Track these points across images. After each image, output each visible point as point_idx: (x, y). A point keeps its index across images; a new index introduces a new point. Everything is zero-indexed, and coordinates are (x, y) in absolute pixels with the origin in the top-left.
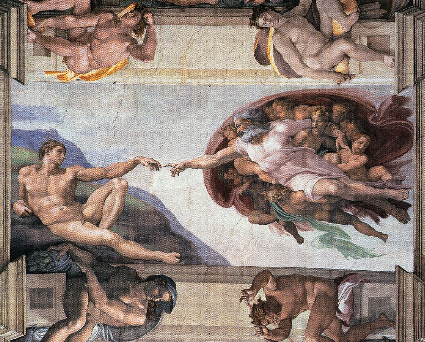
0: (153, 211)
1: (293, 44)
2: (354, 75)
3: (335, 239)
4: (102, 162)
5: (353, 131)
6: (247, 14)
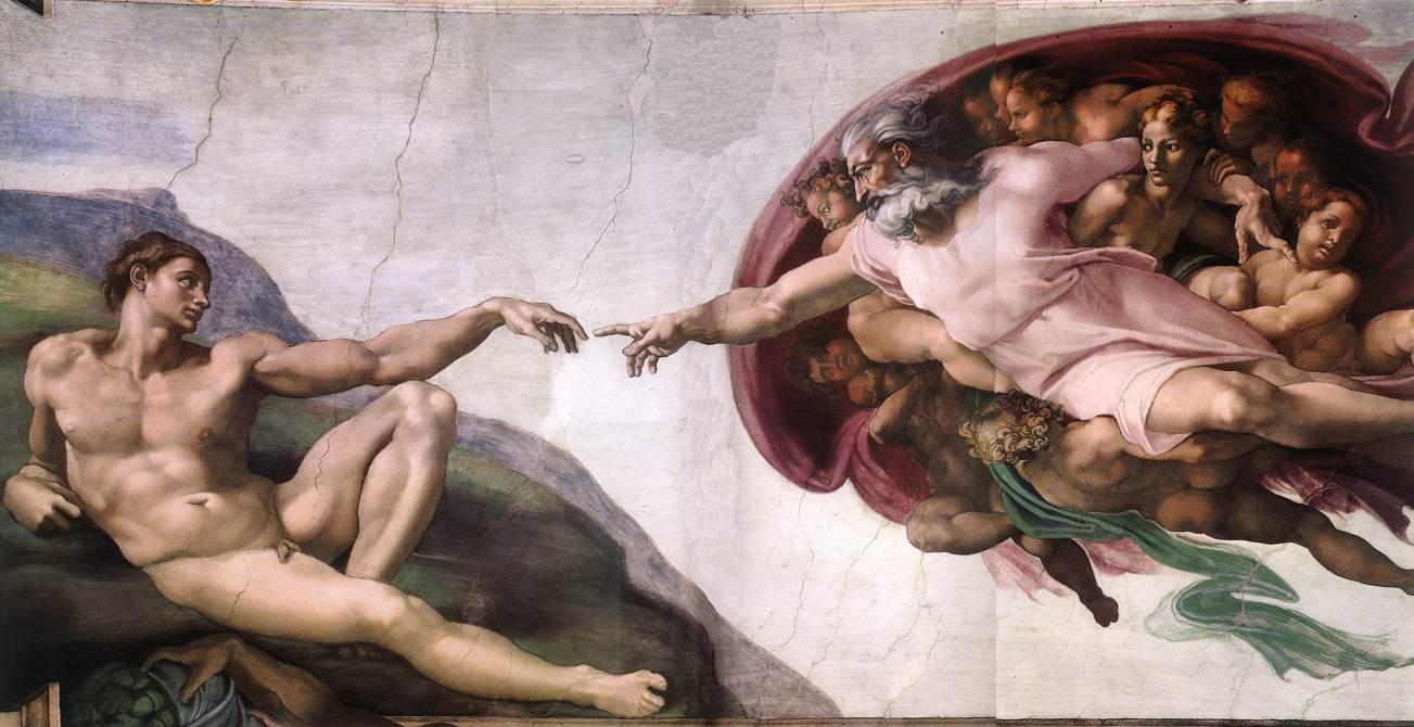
3: (1238, 605)
4: (353, 320)
5: (1299, 180)
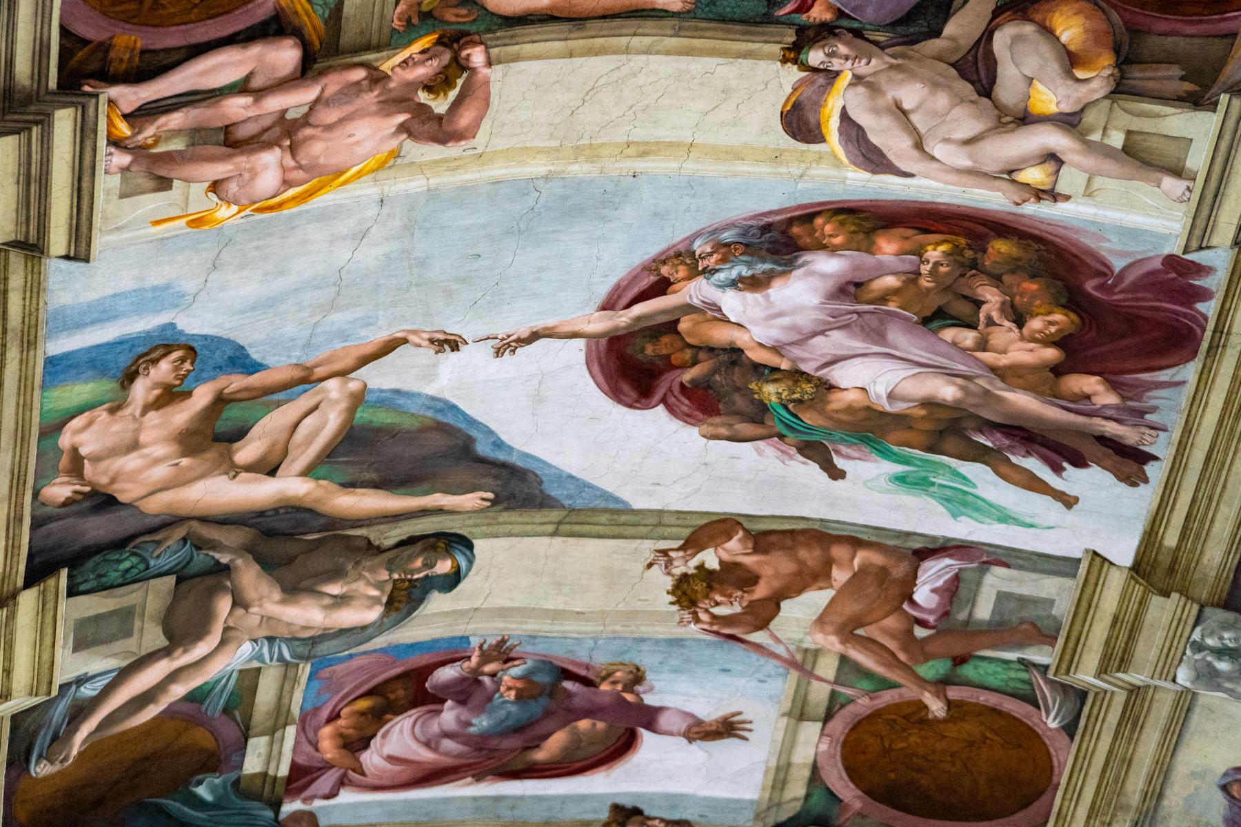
0: (429, 422)
1: (905, 113)
2: (1067, 198)
3: (933, 484)
4: (298, 354)
5: (1034, 297)
6: (778, 39)
